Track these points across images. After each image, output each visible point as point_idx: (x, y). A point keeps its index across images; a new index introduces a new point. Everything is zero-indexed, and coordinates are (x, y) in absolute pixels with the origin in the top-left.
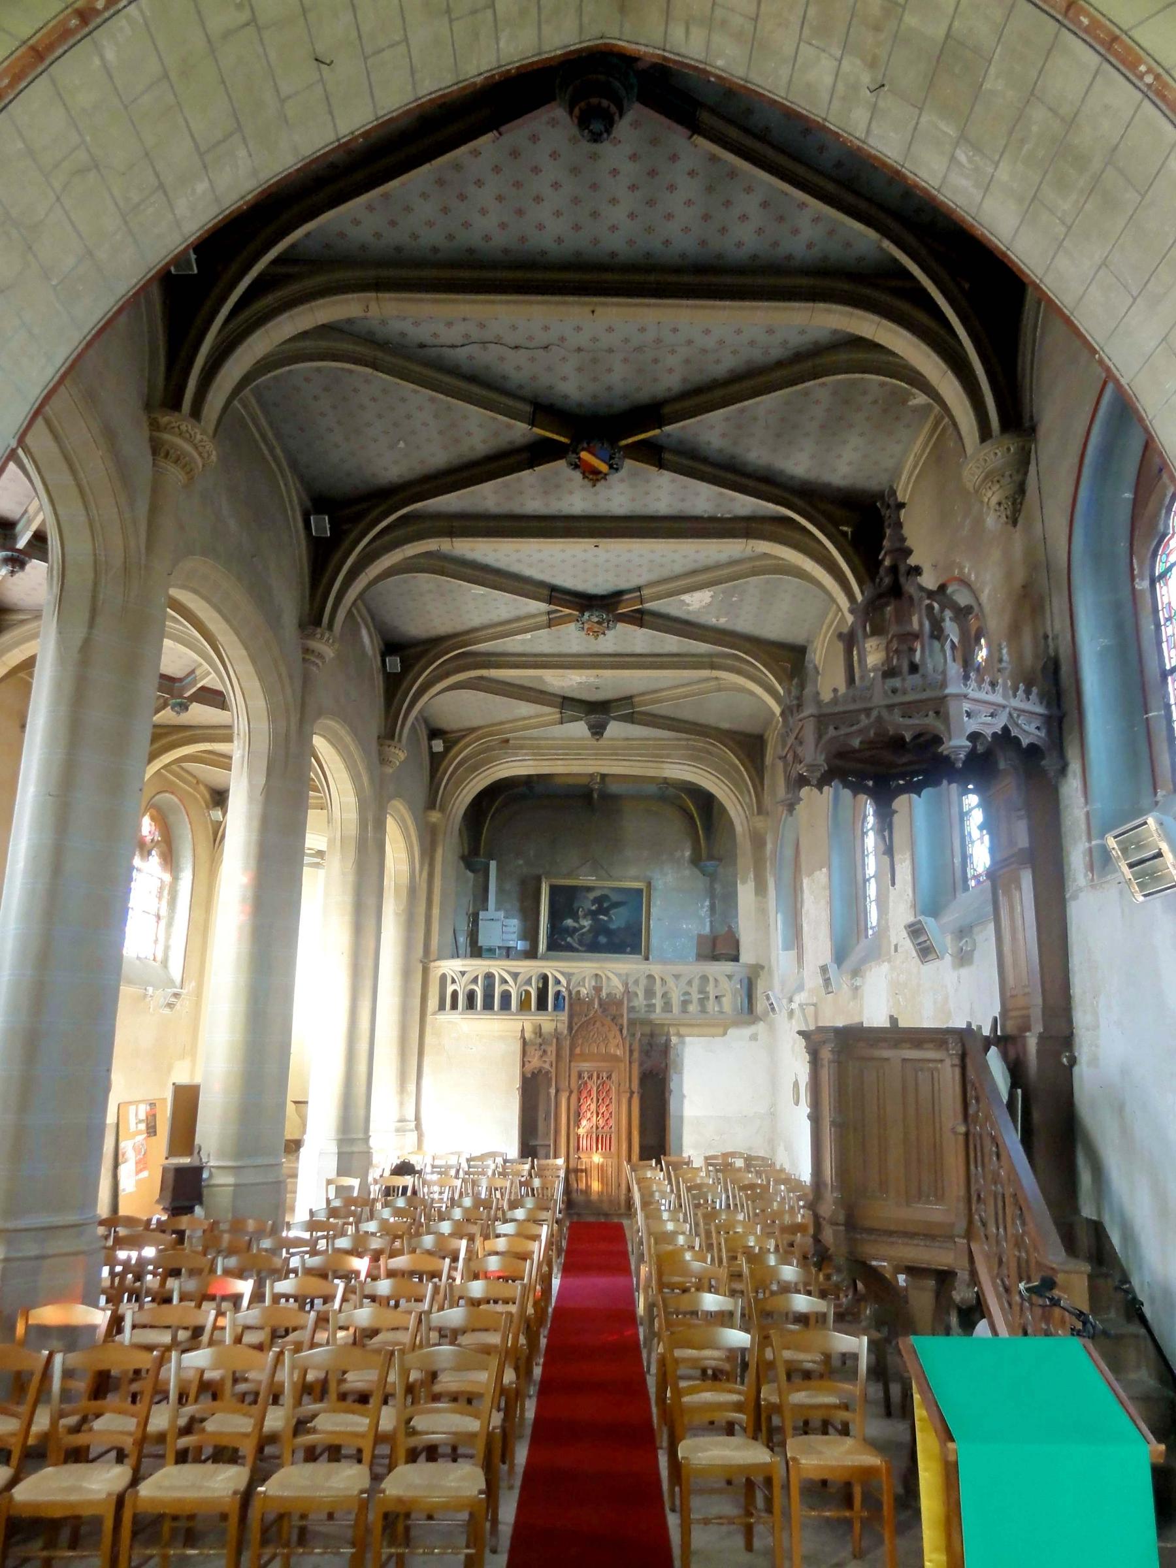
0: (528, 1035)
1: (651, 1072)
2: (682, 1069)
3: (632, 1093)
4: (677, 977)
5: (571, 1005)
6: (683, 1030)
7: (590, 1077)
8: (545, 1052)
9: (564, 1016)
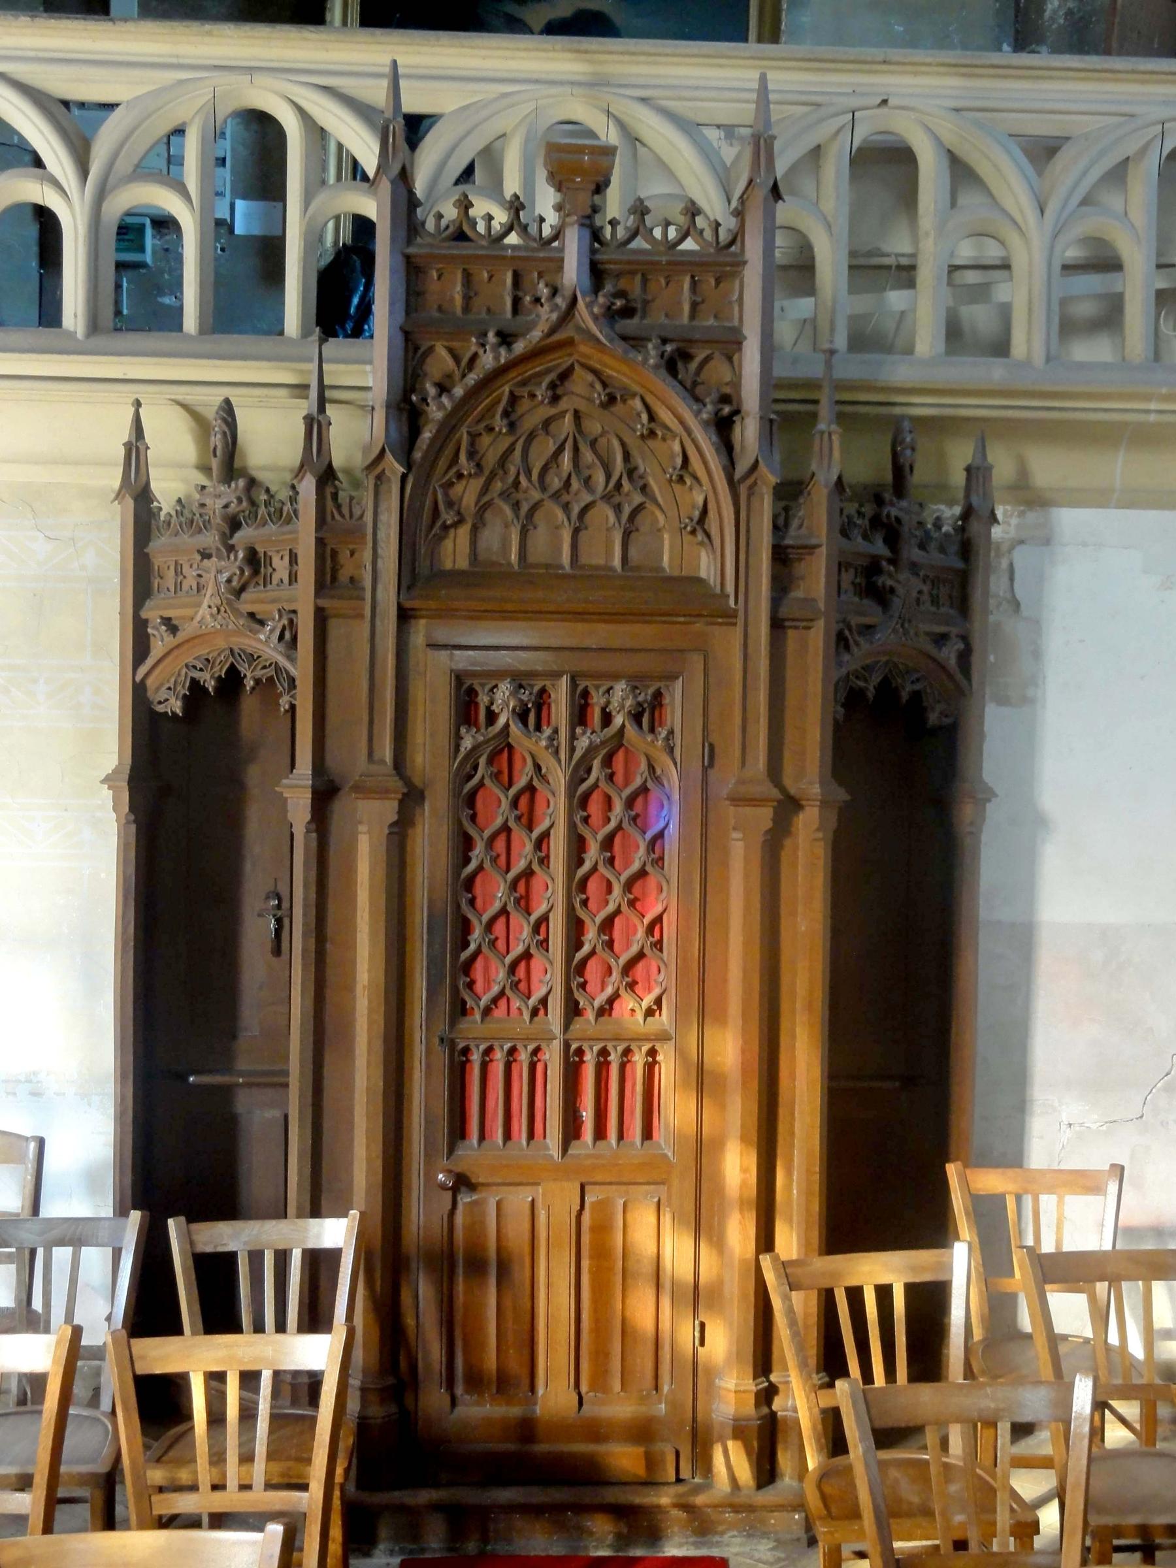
0: (174, 479)
1: (887, 688)
2: (1035, 680)
3: (789, 805)
4: (1043, 152)
5: (413, 271)
6: (1048, 466)
7: (533, 712)
8: (254, 560)
9: (364, 370)
